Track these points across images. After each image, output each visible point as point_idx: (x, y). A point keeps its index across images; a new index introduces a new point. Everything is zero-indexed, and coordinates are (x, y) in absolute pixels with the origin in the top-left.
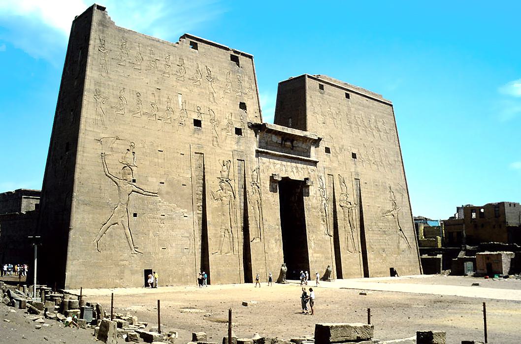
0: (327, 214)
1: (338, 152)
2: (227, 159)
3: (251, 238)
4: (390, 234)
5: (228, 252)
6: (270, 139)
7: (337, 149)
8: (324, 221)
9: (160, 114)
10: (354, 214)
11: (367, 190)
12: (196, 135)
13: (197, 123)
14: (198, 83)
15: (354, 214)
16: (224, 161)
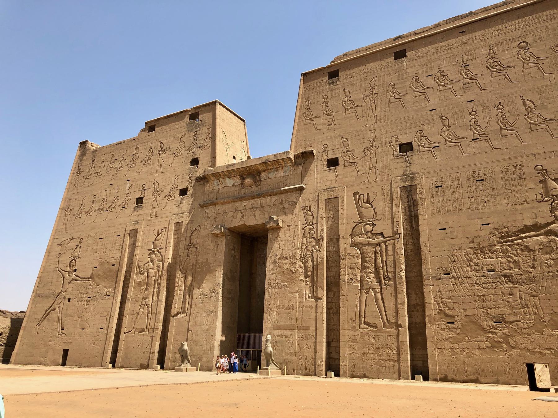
0: (315, 263)
1: (363, 155)
2: (163, 227)
3: (174, 311)
4: (533, 280)
5: (143, 331)
6: (223, 185)
7: (358, 152)
8: (306, 276)
9: (107, 206)
10: (390, 253)
11: (442, 199)
12: (136, 213)
13: (140, 201)
14: (149, 161)
15: (390, 253)
16: (158, 230)
